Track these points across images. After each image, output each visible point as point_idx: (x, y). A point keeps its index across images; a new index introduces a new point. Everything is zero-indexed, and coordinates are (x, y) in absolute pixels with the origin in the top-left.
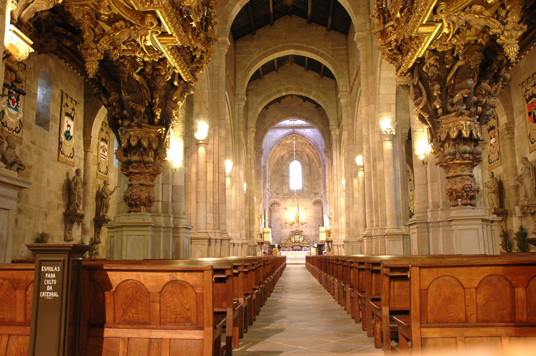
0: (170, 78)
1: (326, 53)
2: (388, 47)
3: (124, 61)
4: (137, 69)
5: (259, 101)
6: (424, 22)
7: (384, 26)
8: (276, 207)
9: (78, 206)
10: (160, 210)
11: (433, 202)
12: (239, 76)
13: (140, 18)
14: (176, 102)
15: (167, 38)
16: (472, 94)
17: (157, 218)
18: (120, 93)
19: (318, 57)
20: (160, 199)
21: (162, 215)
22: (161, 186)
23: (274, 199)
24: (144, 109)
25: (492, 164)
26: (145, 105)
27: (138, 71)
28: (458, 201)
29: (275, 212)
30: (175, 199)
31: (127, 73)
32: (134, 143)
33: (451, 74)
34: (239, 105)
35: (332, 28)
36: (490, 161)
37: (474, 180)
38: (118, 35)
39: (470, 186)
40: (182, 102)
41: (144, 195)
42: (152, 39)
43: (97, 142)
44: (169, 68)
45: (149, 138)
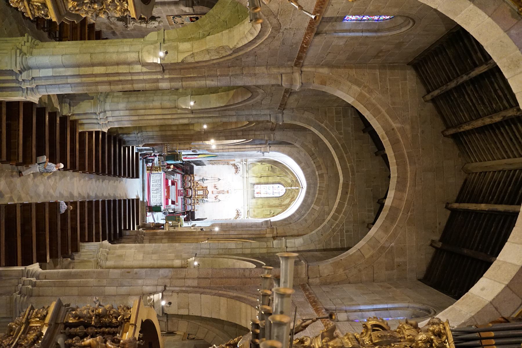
1: (337, 222)
5: (307, 144)
8: (233, 170)
12: (306, 115)
34: (270, 115)
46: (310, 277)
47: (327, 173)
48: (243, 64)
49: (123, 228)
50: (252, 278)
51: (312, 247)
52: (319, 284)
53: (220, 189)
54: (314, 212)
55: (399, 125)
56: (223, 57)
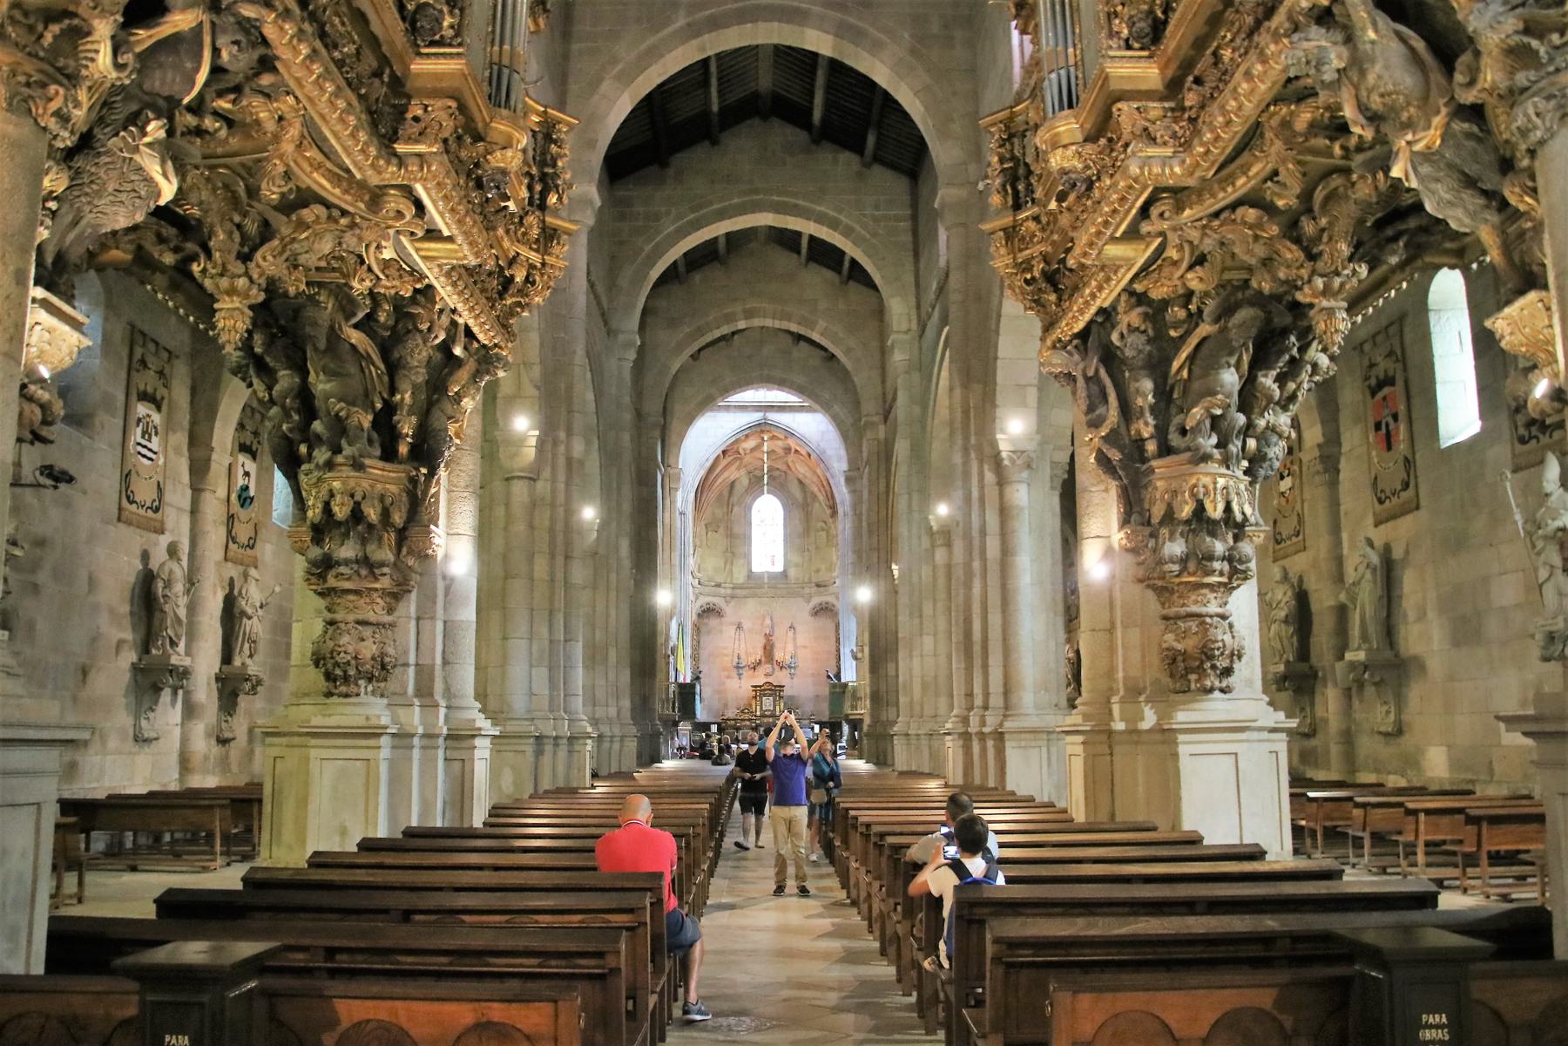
0: (442, 336)
1: (858, 228)
2: (1024, 271)
3: (318, 293)
4: (354, 314)
6: (1118, 235)
7: (1015, 216)
8: (713, 622)
9: (173, 644)
10: (411, 689)
11: (1125, 678)
12: (624, 281)
13: (367, 198)
14: (458, 398)
15: (439, 246)
16: (1234, 408)
17: (401, 711)
18: (304, 373)
20: (412, 659)
21: (416, 701)
22: (413, 623)
23: (708, 599)
24: (370, 417)
25: (1283, 545)
26: (373, 407)
27: (354, 320)
28: (1189, 681)
29: (709, 632)
30: (450, 657)
31: (326, 324)
32: (341, 511)
33: (1184, 355)
34: (620, 359)
35: (877, 159)
36: (1278, 537)
37: (1231, 626)
38: (307, 238)
39: (1220, 644)
40: (473, 399)
41: (369, 650)
42: (399, 248)
43: (227, 460)
44: (441, 311)
45: (382, 498)
51: (909, 278)
53: (759, 654)
55: (682, 12)
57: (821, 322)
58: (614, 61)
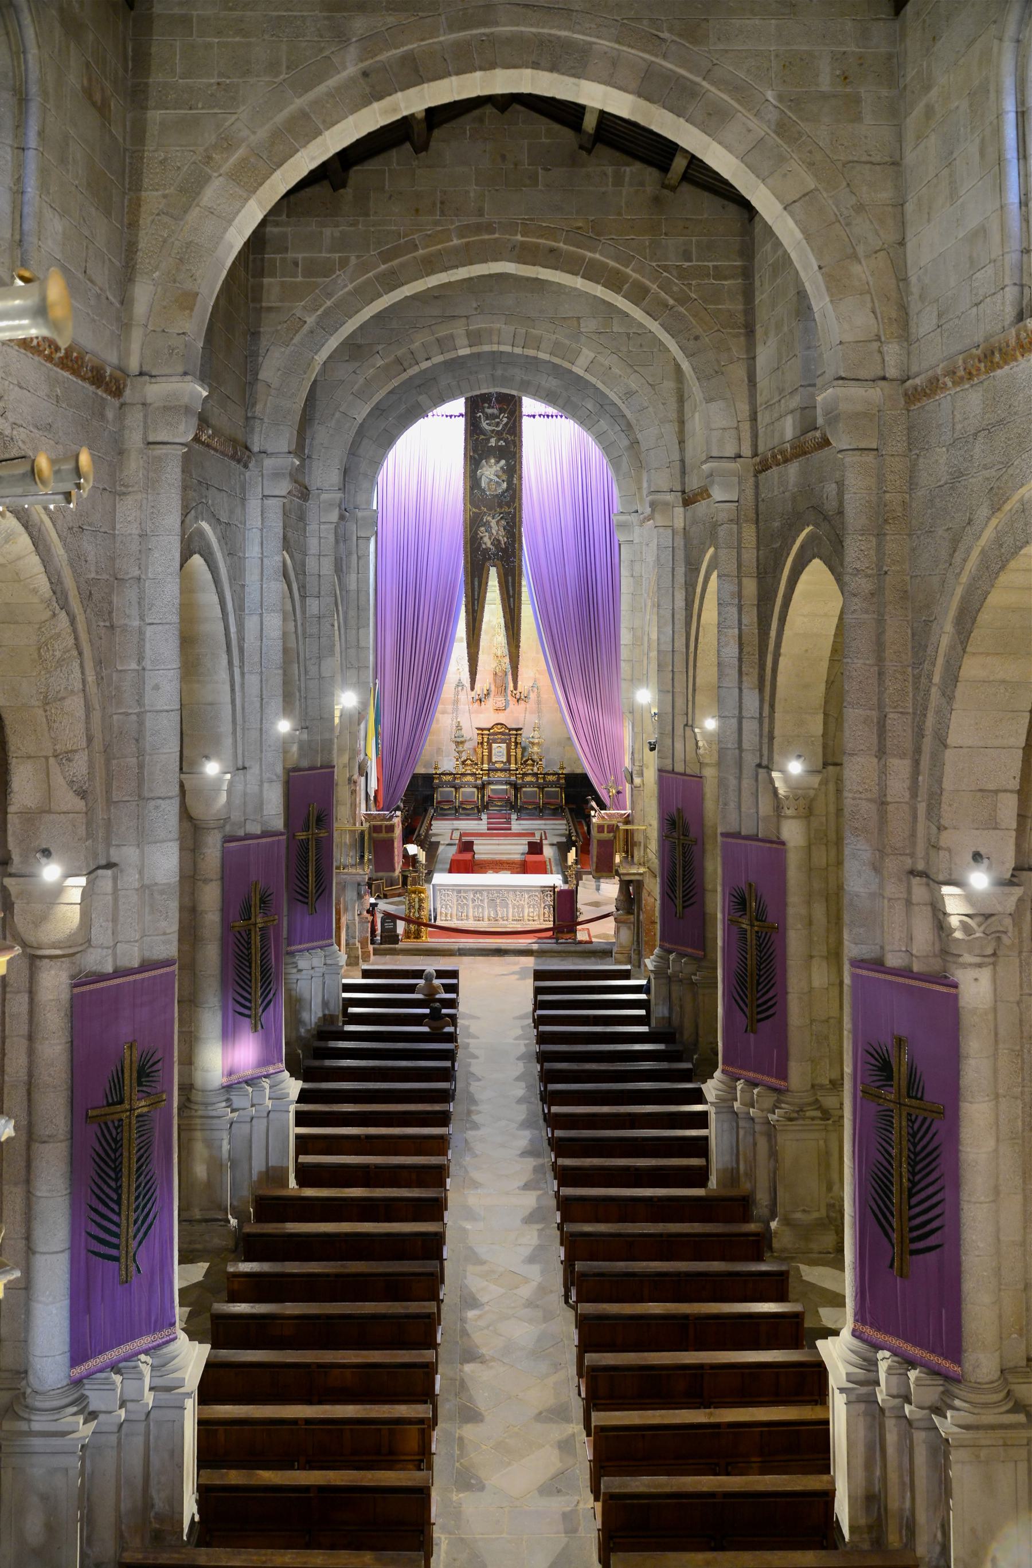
5: (361, 381)
19: (620, 298)
46: (881, 374)
47: (467, 317)
48: (105, 576)
49: (644, 1029)
50: (880, 568)
52: (905, 344)
54: (602, 365)
55: (353, 51)
56: (77, 646)
57: (585, 351)
58: (227, 143)
